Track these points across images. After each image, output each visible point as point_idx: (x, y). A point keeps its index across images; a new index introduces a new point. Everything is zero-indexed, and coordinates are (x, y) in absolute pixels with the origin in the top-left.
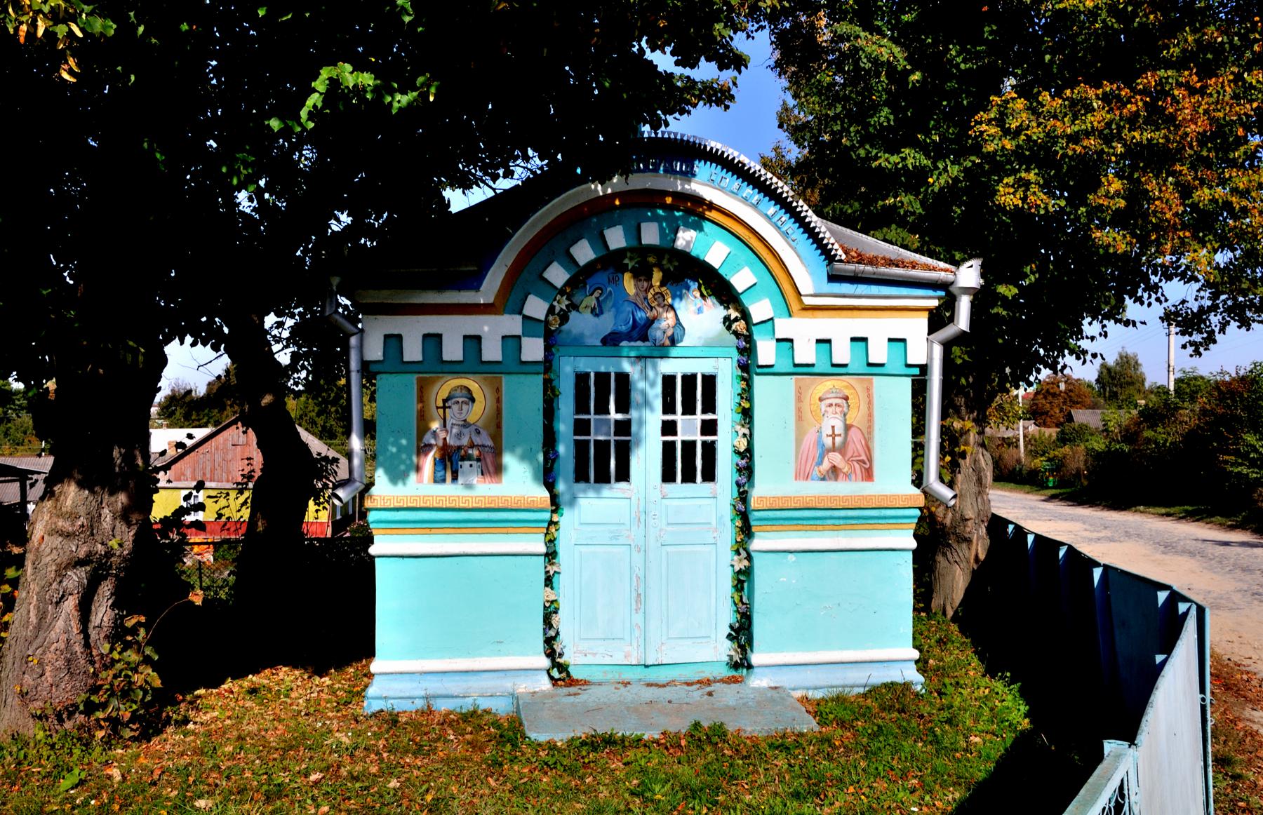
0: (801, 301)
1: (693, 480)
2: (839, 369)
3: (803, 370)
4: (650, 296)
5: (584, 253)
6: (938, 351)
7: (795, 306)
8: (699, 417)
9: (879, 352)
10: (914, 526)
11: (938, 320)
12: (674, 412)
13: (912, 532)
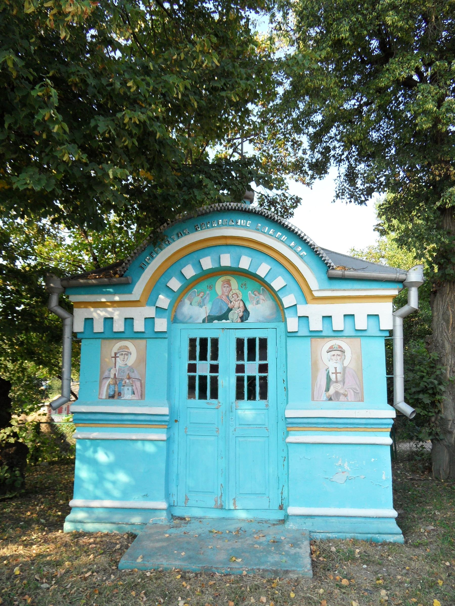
0: (312, 295)
1: (254, 399)
2: (338, 334)
3: (316, 335)
4: (230, 295)
5: (189, 272)
6: (399, 322)
7: (309, 298)
8: (258, 362)
9: (361, 323)
10: (390, 430)
11: (400, 301)
12: (243, 360)
13: (389, 433)
